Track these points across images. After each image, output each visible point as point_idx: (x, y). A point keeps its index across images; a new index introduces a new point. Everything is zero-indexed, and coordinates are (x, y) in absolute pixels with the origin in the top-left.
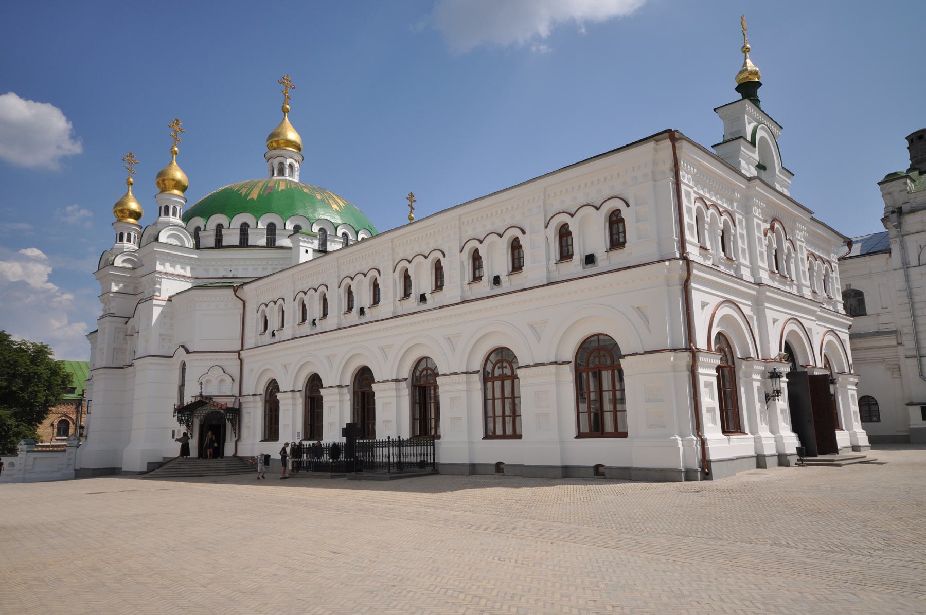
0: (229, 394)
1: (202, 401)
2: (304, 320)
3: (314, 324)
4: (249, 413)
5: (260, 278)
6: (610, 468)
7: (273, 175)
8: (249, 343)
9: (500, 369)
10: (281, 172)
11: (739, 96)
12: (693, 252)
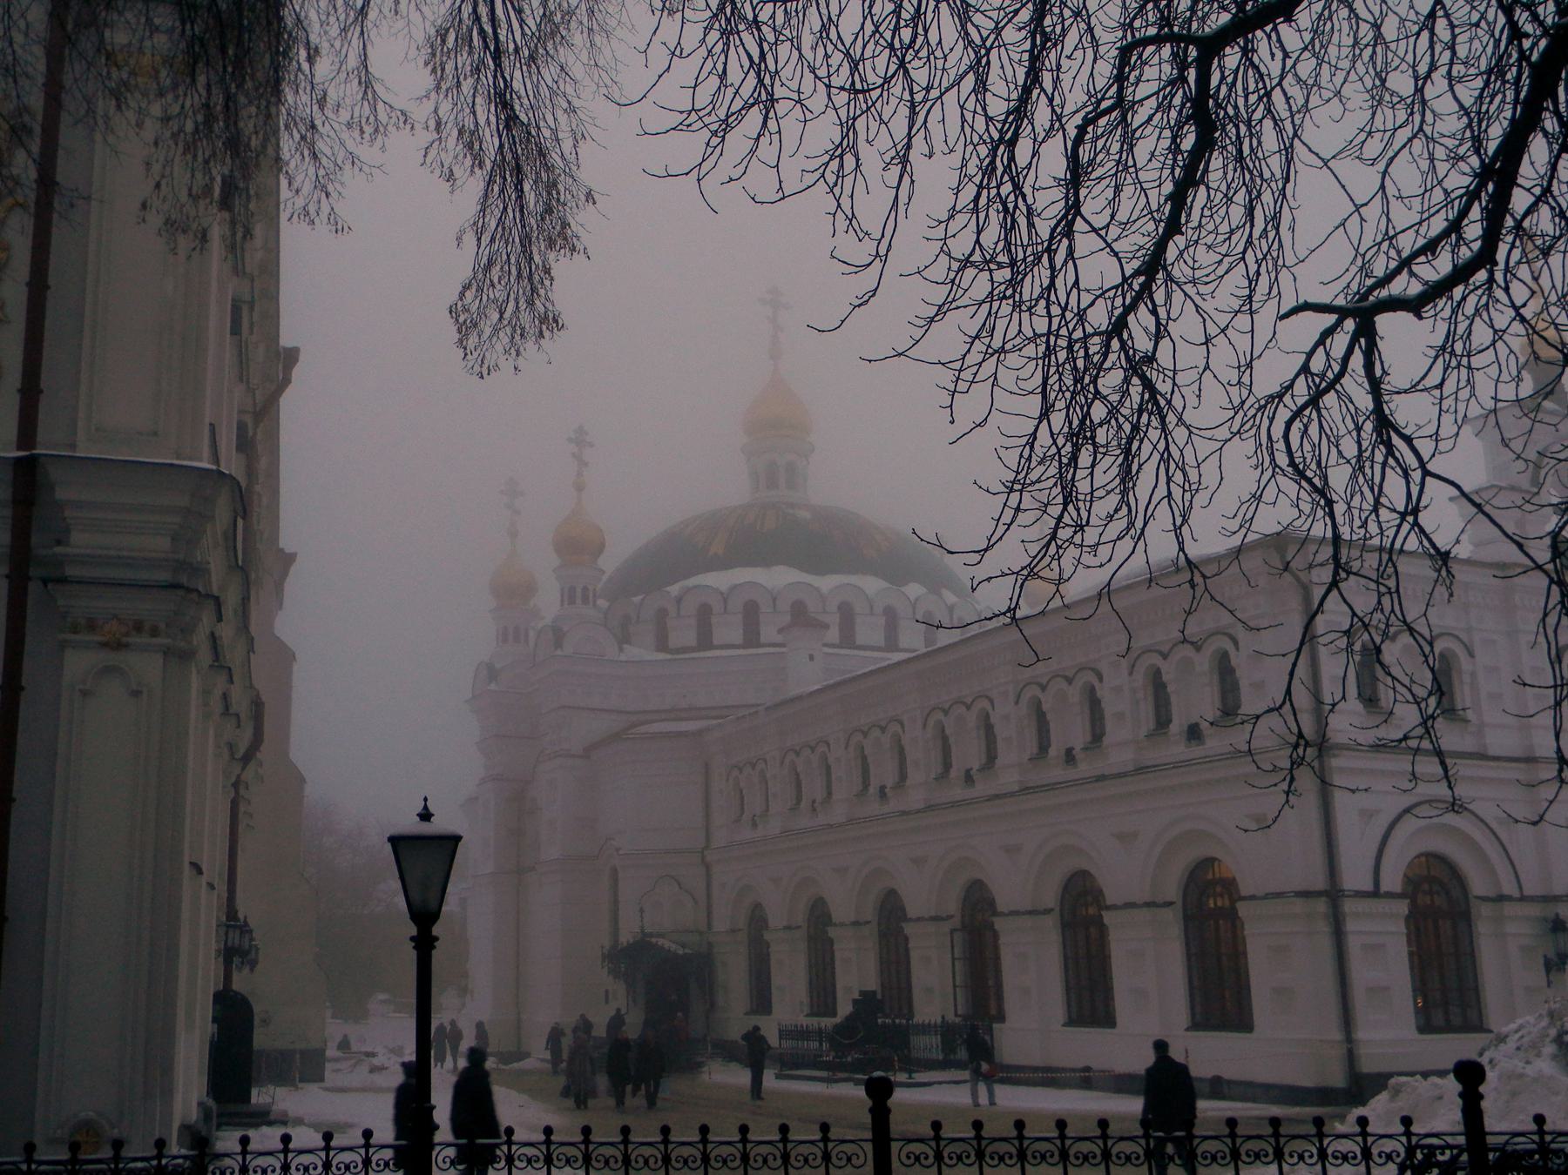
2: (799, 800)
3: (814, 810)
6: (1229, 1082)
9: (1082, 914)
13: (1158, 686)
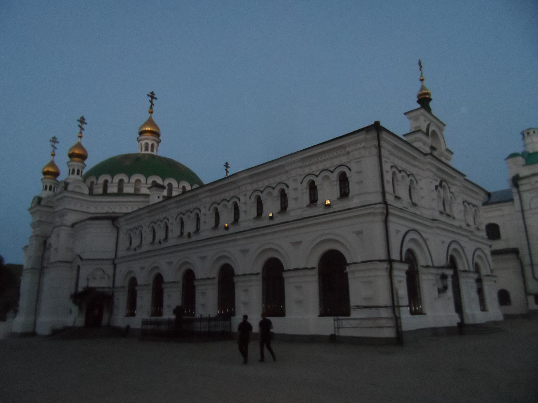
0: (107, 286)
1: (89, 291)
3: (160, 242)
4: (118, 299)
5: (127, 214)
7: (142, 150)
8: (120, 254)
10: (146, 149)
11: (419, 106)
12: (390, 199)
13: (313, 188)
